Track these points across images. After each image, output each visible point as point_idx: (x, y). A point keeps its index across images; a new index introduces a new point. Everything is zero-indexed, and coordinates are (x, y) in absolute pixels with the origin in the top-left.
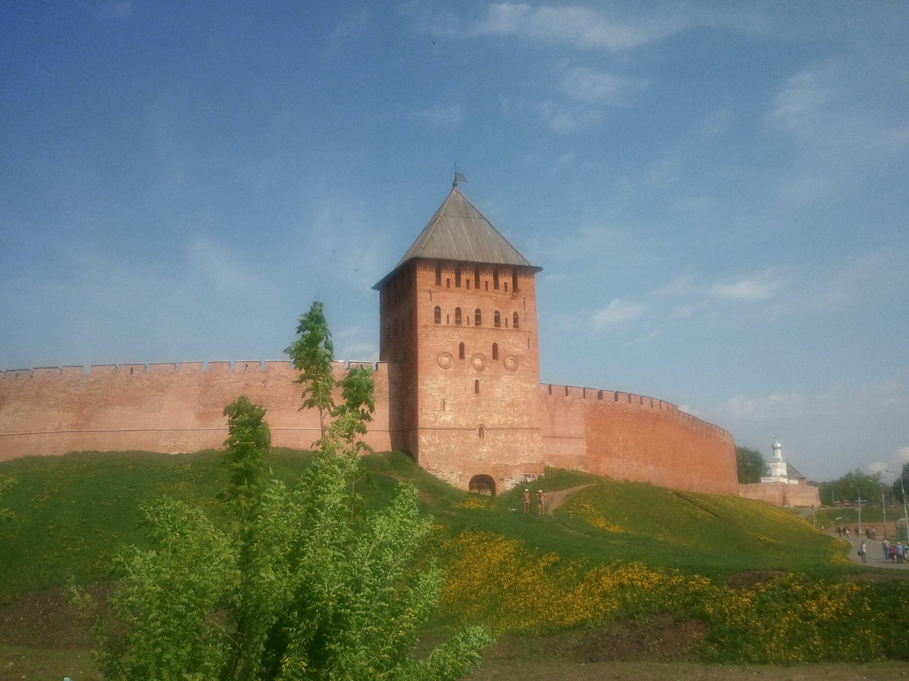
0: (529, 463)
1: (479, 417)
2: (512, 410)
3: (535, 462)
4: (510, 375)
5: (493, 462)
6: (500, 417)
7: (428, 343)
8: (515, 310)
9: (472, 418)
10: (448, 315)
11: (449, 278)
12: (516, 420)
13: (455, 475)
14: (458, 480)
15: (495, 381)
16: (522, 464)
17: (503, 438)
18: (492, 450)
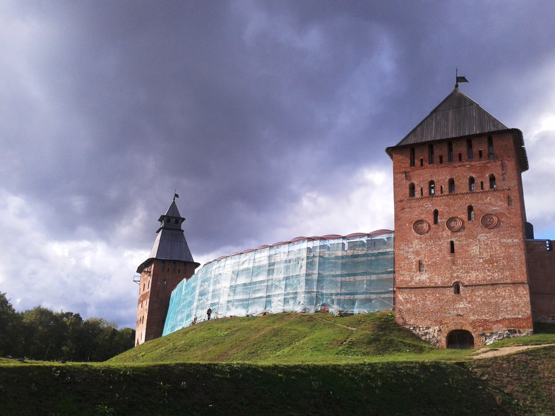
0: (512, 319)
1: (455, 275)
2: (491, 266)
3: (520, 316)
4: (487, 233)
5: (471, 318)
6: (478, 273)
7: (404, 215)
9: (448, 276)
10: (422, 189)
11: (422, 158)
12: (496, 274)
15: (471, 240)
16: (505, 319)
17: (482, 294)
18: (470, 305)
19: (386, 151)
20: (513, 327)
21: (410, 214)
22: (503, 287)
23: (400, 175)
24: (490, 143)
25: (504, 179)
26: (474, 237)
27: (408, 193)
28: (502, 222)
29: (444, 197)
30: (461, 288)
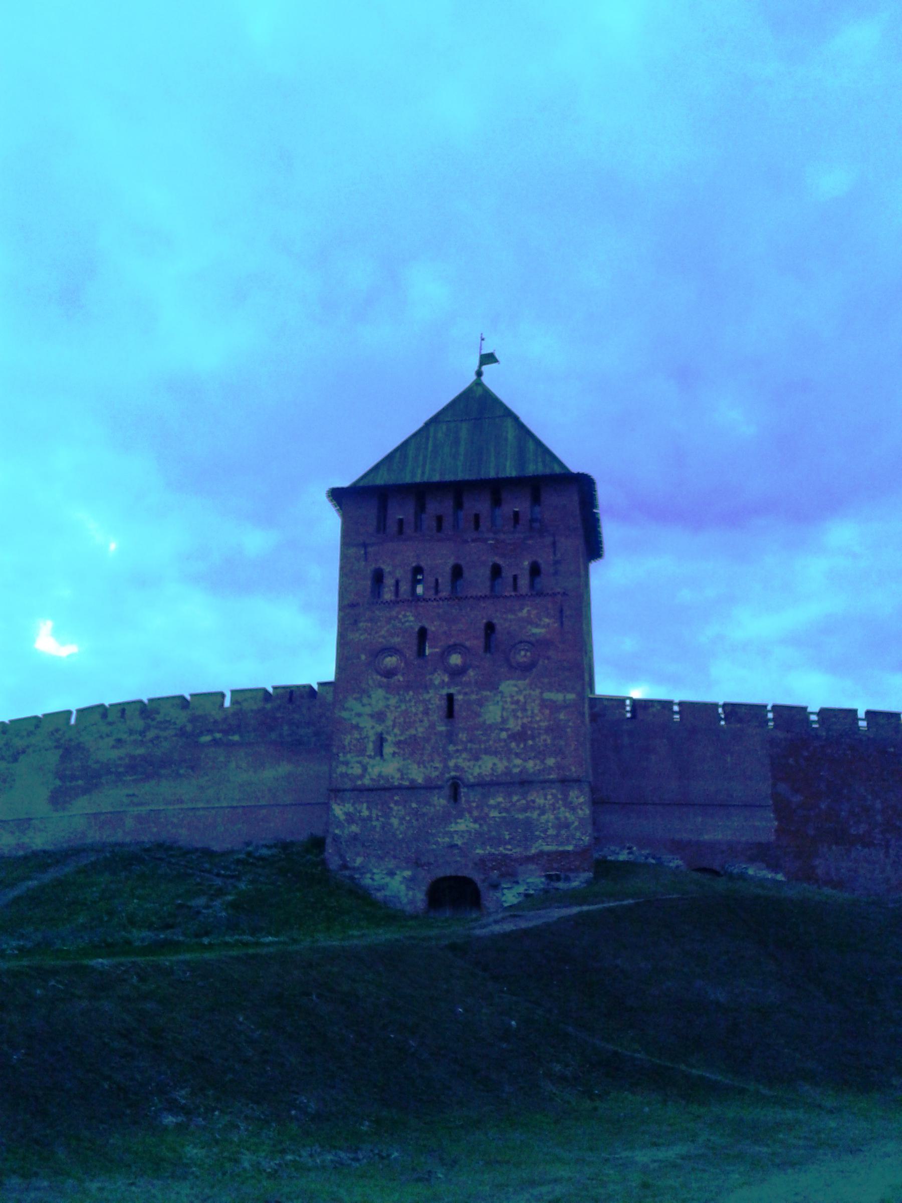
1: (451, 763)
2: (522, 746)
3: (570, 848)
4: (519, 679)
8: (535, 558)
10: (397, 583)
11: (401, 517)
12: (530, 764)
13: (398, 878)
14: (403, 887)
15: (488, 693)
16: (541, 854)
19: (328, 496)
20: (556, 870)
22: (543, 789)
24: (536, 500)
26: (494, 687)
27: (369, 590)
28: (548, 658)
29: (441, 602)
30: (463, 790)
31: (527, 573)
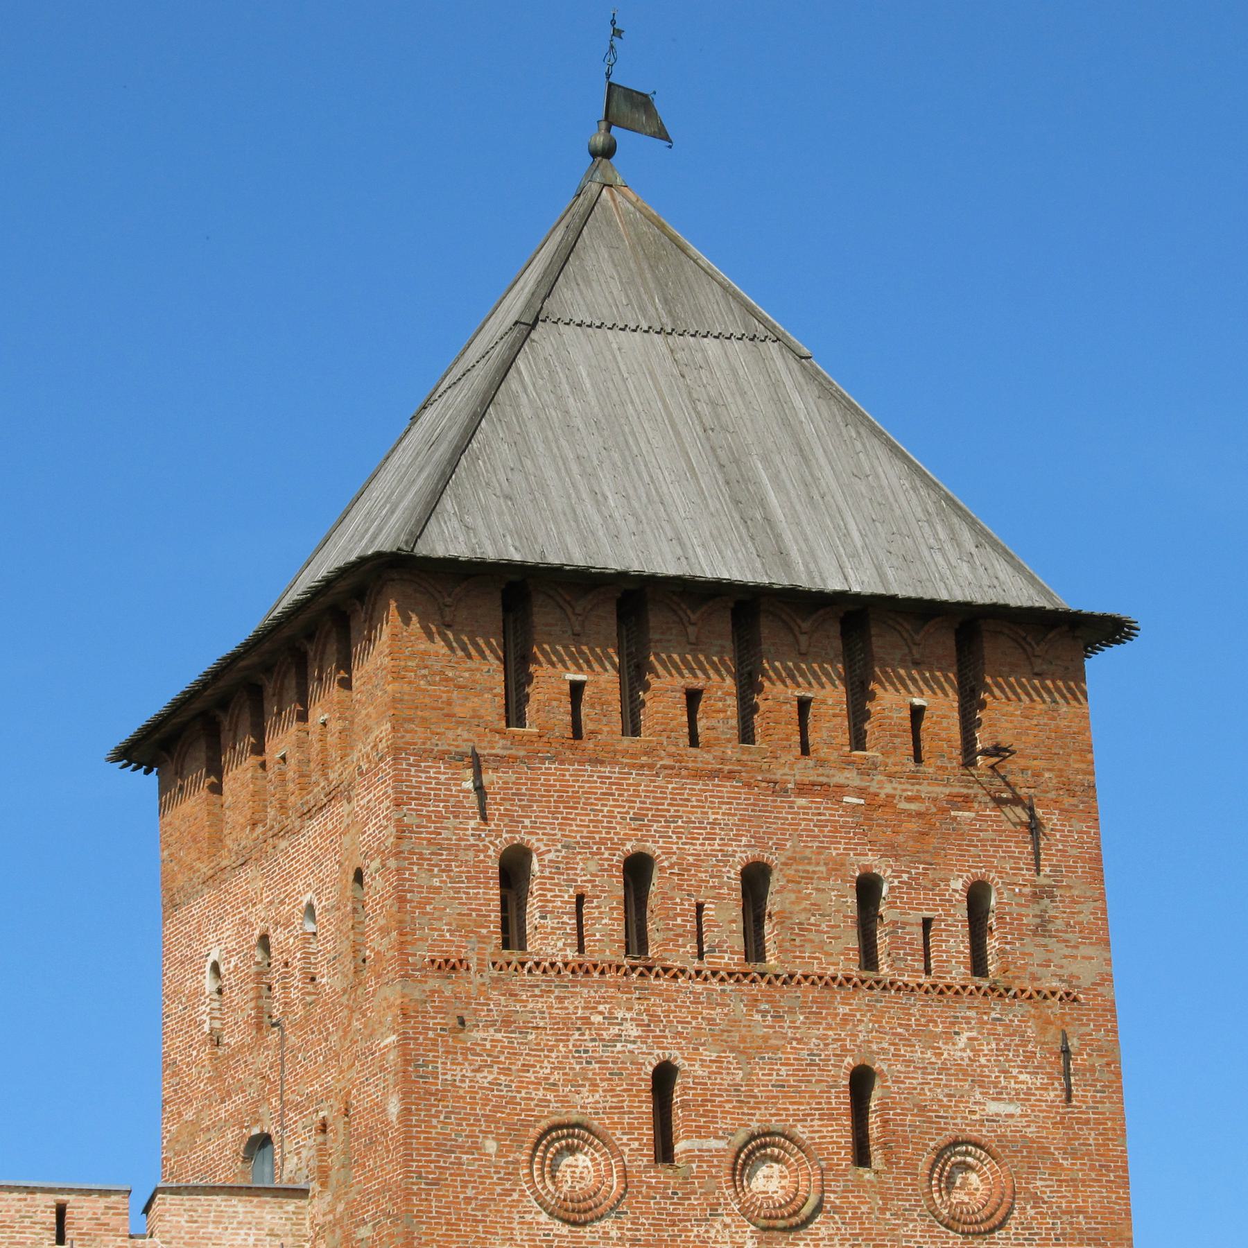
10: (580, 899)
21: (506, 1071)
23: (441, 772)
25: (1042, 927)
28: (1036, 1200)
29: (715, 984)
31: (962, 913)
